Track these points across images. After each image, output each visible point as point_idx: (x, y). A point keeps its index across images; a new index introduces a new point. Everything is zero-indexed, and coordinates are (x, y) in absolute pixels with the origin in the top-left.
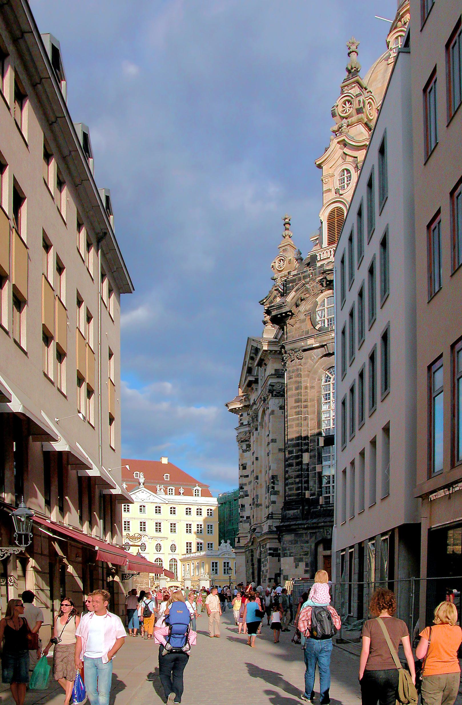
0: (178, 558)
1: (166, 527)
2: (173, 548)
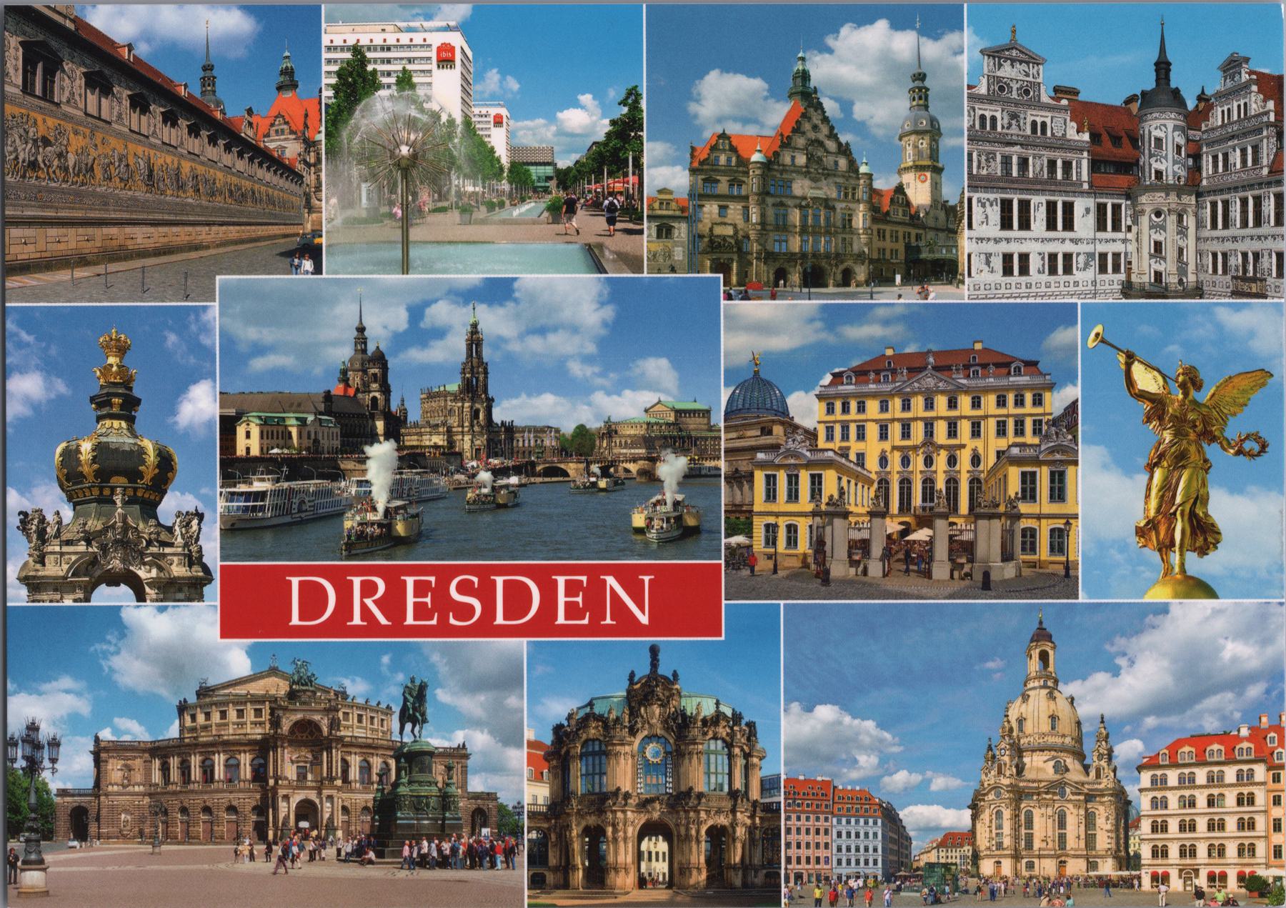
2: (976, 460)
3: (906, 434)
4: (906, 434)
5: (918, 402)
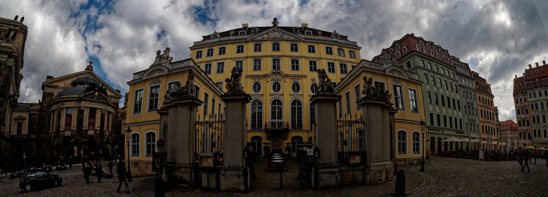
3: (257, 67)
4: (257, 67)
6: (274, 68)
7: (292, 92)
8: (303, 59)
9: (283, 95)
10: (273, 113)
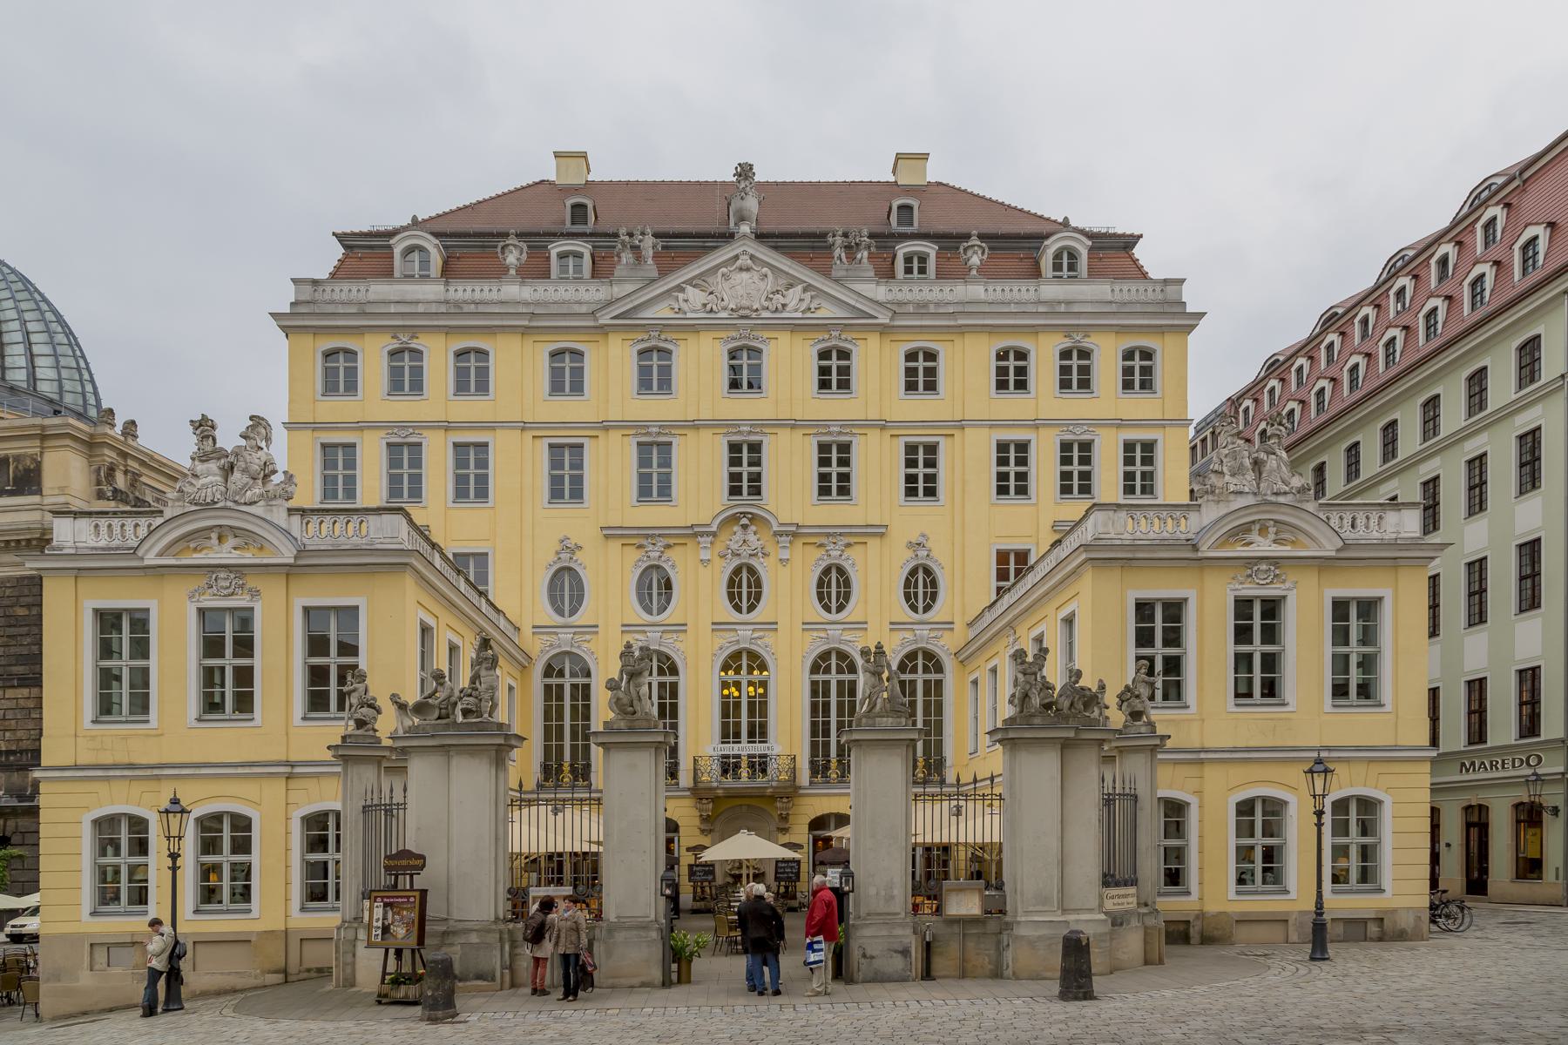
0: (945, 646)
1: (877, 466)
2: (921, 586)
3: (654, 482)
4: (654, 482)
5: (700, 364)
6: (735, 491)
7: (816, 612)
8: (874, 435)
9: (772, 626)
10: (729, 708)
